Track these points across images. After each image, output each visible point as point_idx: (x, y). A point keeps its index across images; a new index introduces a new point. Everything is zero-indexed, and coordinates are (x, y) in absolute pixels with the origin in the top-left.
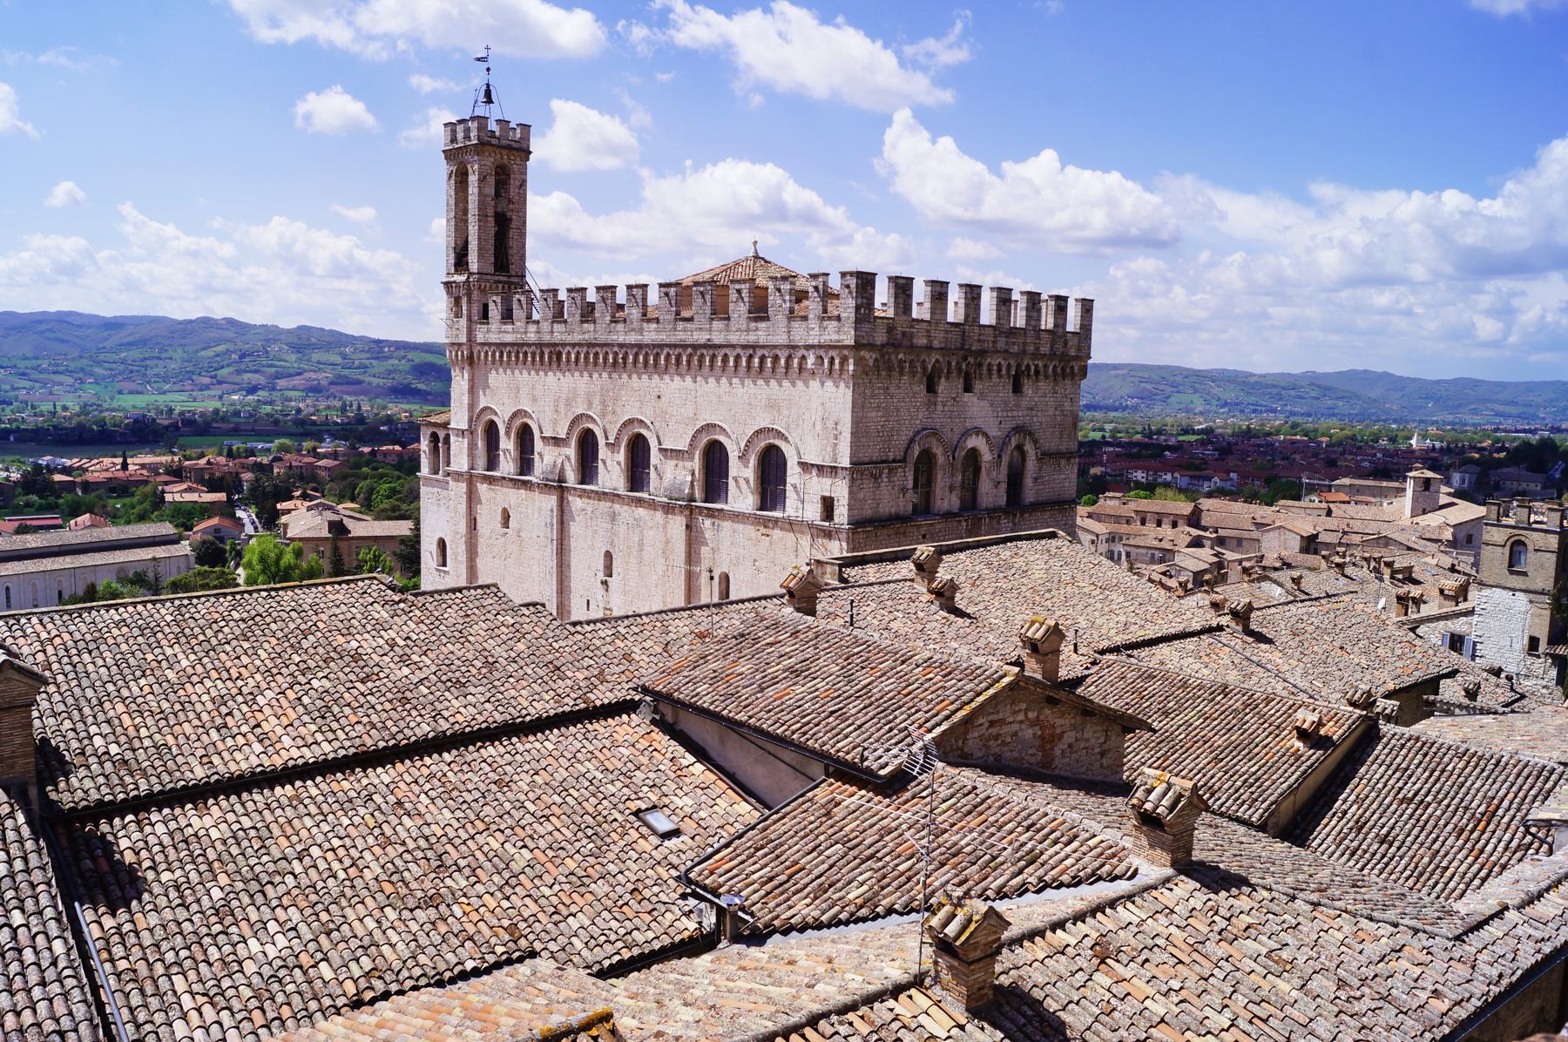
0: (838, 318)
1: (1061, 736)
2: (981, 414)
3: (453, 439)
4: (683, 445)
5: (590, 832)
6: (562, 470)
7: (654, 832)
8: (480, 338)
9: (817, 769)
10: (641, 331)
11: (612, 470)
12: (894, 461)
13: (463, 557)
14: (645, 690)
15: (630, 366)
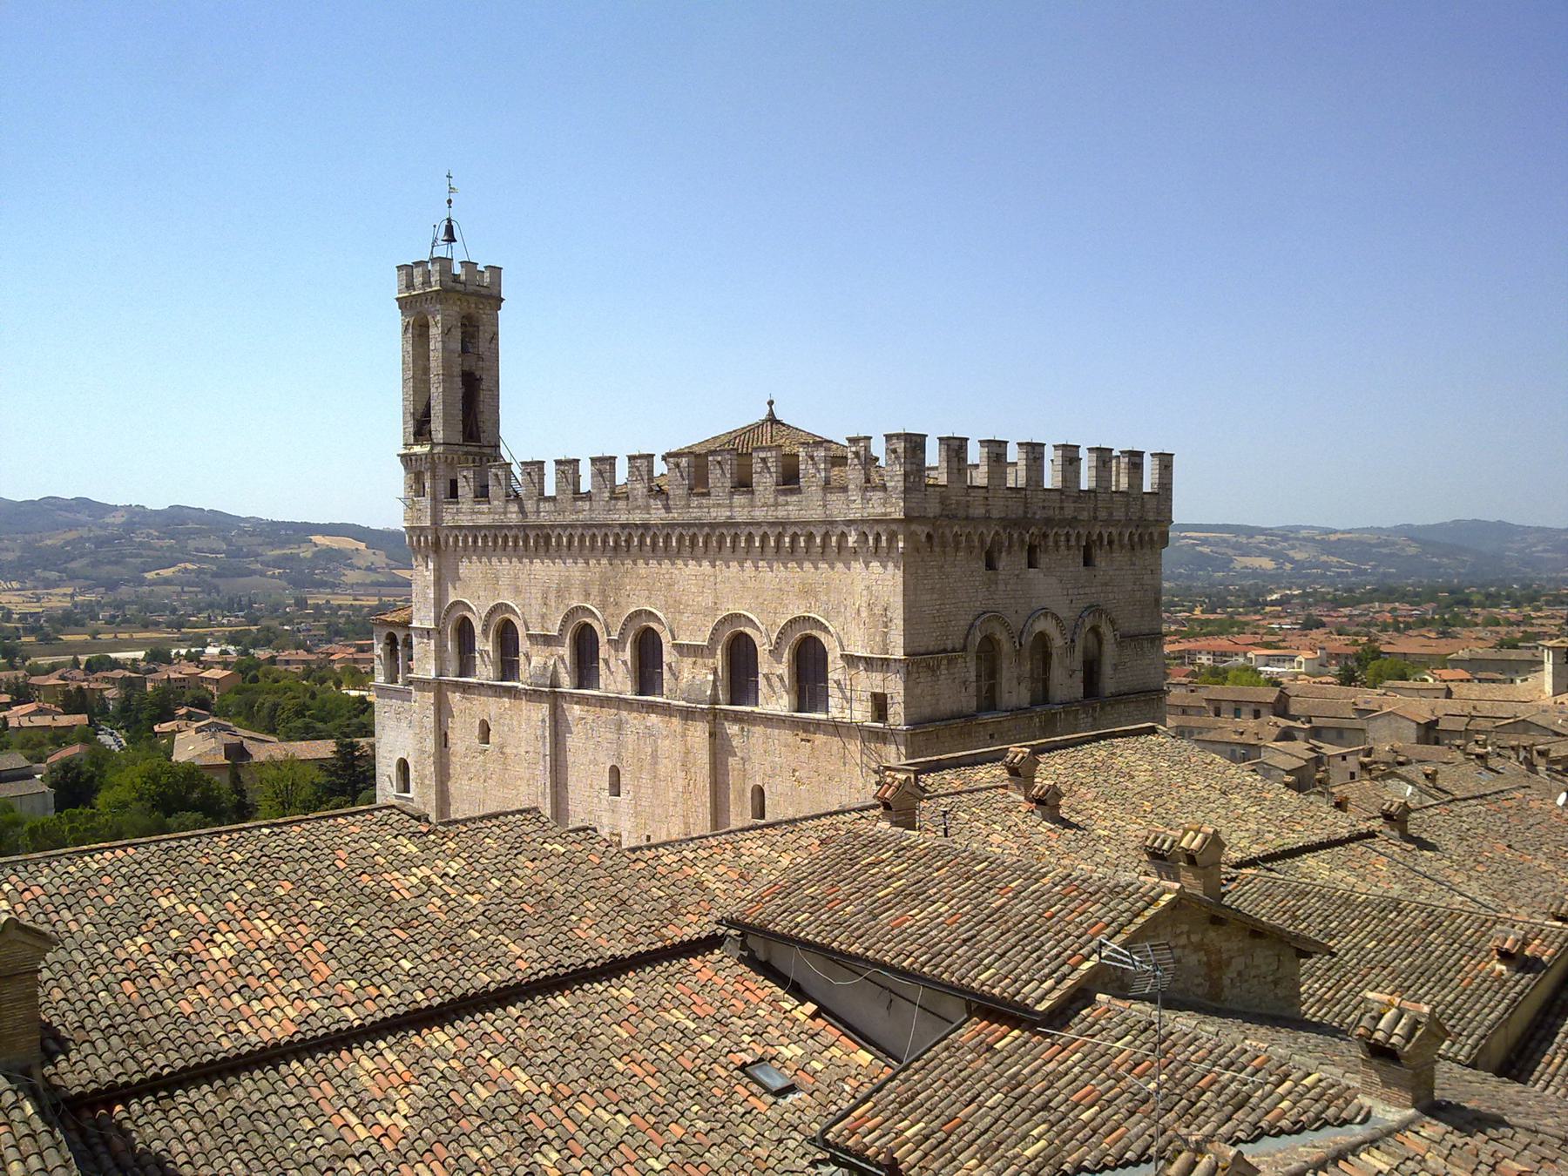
0: (884, 488)
1: (1229, 964)
2: (1049, 592)
3: (415, 640)
4: (702, 639)
5: (692, 1092)
6: (555, 671)
7: (768, 1090)
8: (448, 520)
9: (952, 1007)
10: (647, 508)
11: (616, 675)
12: (954, 650)
13: (431, 781)
14: (732, 923)
15: (634, 550)
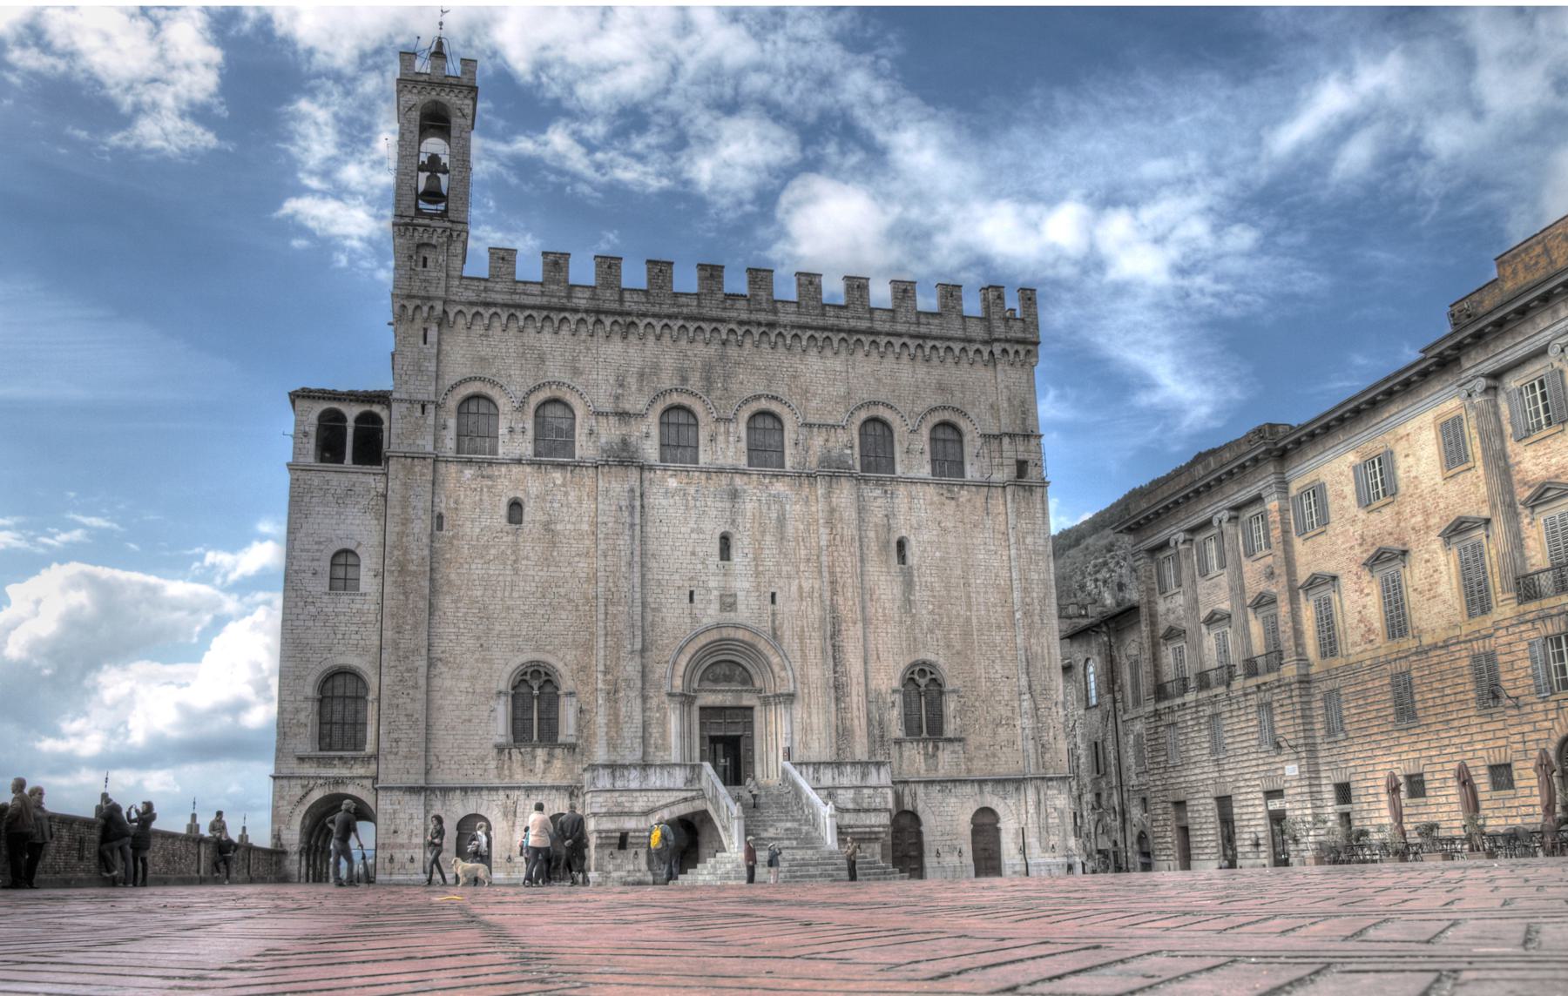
4: (839, 416)
10: (775, 312)
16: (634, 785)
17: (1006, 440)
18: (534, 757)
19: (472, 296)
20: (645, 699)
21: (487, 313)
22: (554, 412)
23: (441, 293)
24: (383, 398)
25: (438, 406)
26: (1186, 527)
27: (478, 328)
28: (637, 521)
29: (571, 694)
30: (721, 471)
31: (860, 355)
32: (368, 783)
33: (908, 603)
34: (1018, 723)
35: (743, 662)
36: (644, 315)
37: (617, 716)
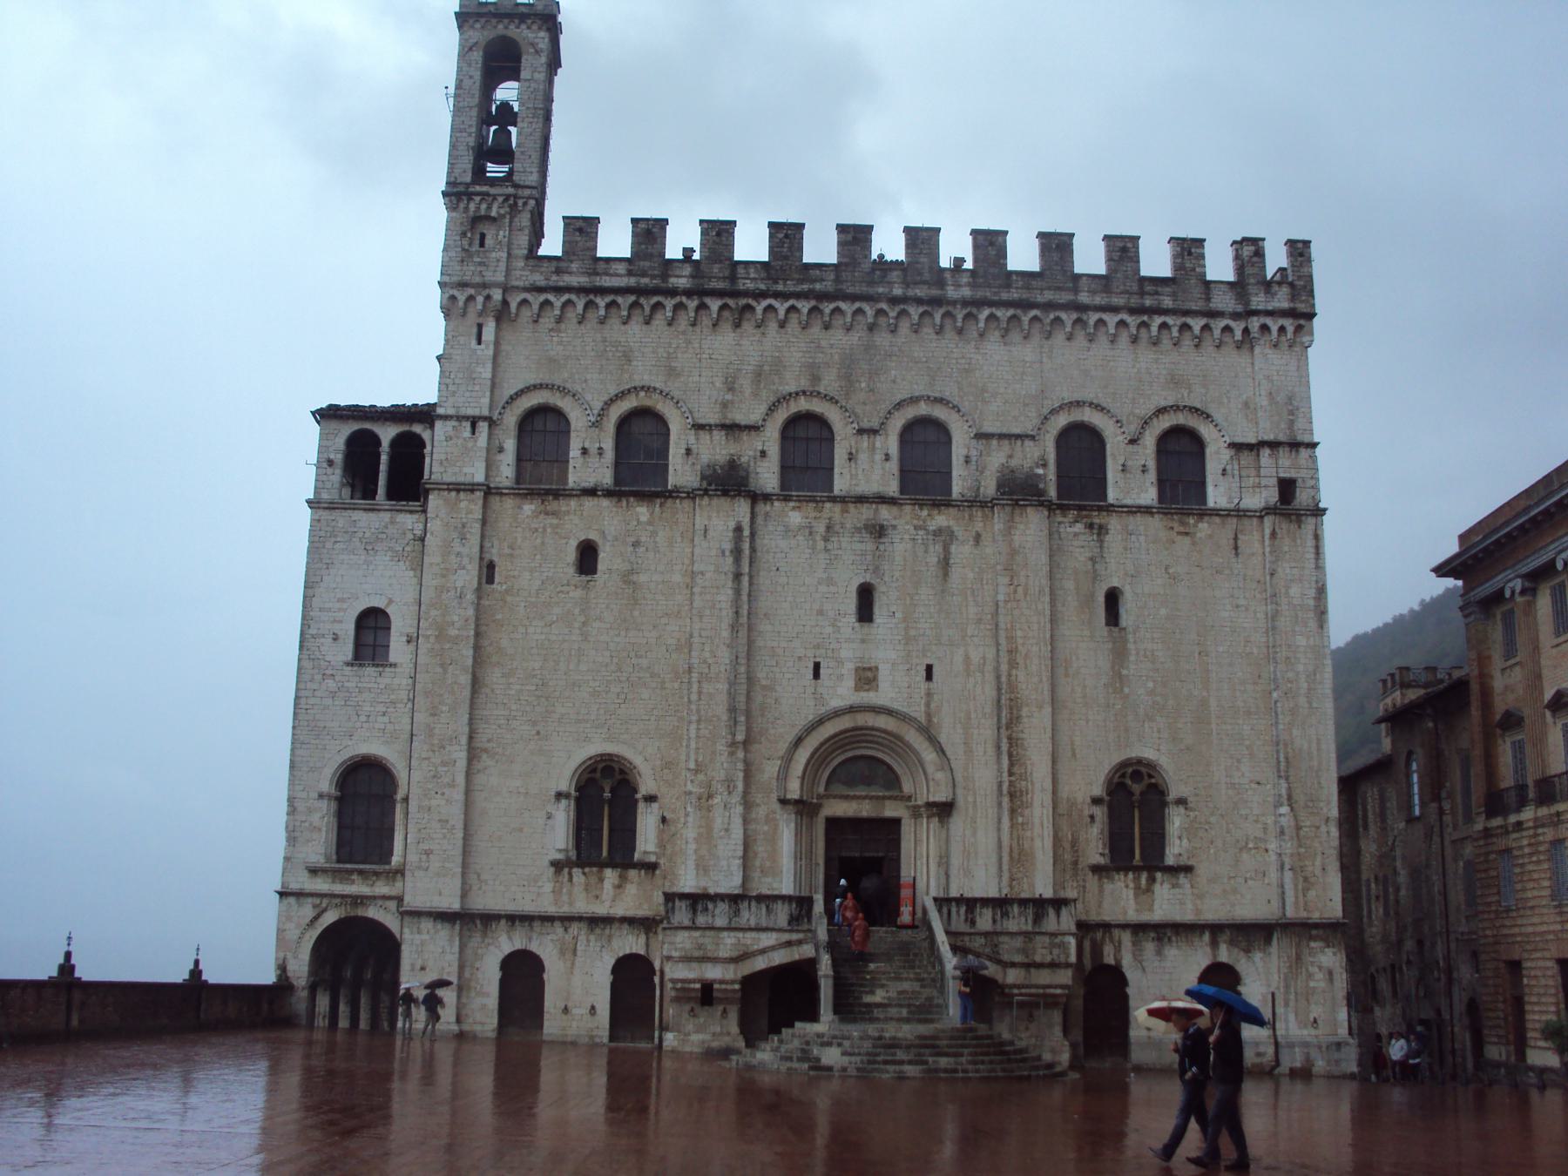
16: (720, 922)
17: (1266, 452)
18: (601, 880)
19: (538, 279)
20: (748, 804)
21: (558, 301)
22: (641, 427)
23: (500, 278)
24: (425, 414)
25: (492, 422)
26: (1525, 570)
27: (547, 321)
28: (746, 569)
29: (651, 799)
30: (861, 499)
31: (1059, 338)
32: (392, 905)
33: (1118, 679)
34: (1272, 846)
35: (888, 759)
36: (762, 295)
37: (709, 828)
